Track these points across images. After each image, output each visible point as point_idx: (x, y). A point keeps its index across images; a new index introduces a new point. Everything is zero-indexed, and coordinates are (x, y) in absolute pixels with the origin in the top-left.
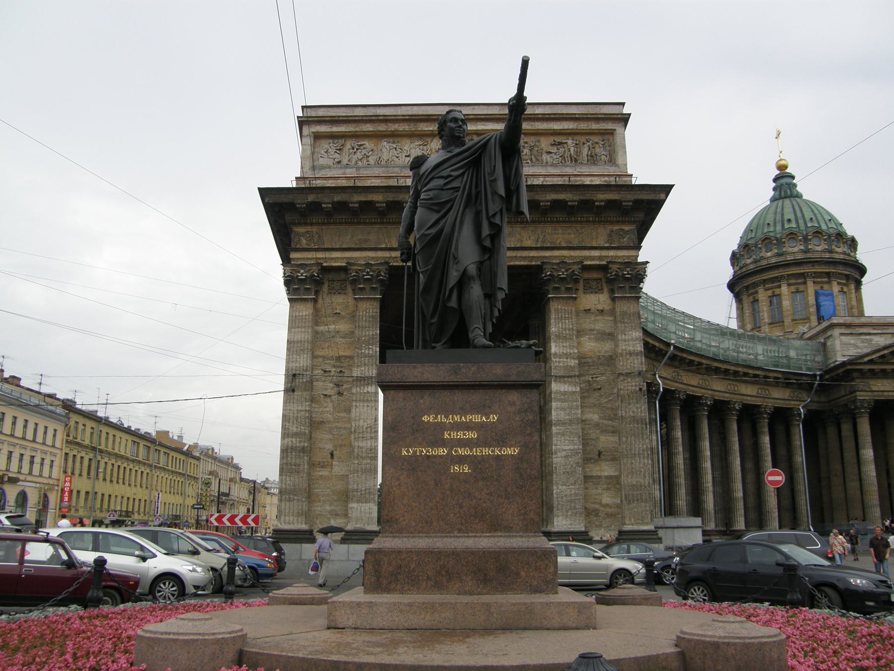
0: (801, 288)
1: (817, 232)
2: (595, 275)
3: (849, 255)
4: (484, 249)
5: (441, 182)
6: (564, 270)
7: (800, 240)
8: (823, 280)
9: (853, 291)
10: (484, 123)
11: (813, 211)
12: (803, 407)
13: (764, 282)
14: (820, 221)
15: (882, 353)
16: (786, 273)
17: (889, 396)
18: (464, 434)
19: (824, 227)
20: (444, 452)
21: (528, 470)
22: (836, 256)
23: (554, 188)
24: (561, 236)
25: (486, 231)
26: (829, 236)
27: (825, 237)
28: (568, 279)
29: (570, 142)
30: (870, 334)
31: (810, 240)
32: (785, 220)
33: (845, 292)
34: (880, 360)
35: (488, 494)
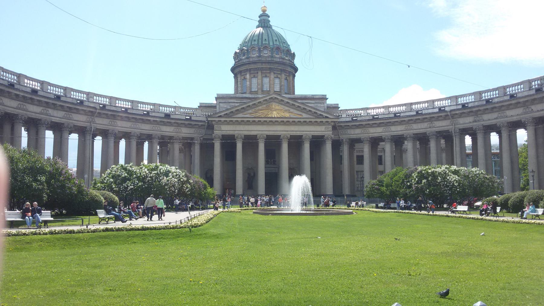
0: (256, 75)
1: (266, 47)
3: (284, 59)
7: (257, 51)
8: (267, 71)
11: (268, 35)
12: (200, 138)
13: (241, 72)
16: (249, 68)
17: (230, 133)
19: (271, 44)
22: (275, 60)
30: (234, 102)
31: (262, 51)
32: (253, 40)
33: (279, 78)
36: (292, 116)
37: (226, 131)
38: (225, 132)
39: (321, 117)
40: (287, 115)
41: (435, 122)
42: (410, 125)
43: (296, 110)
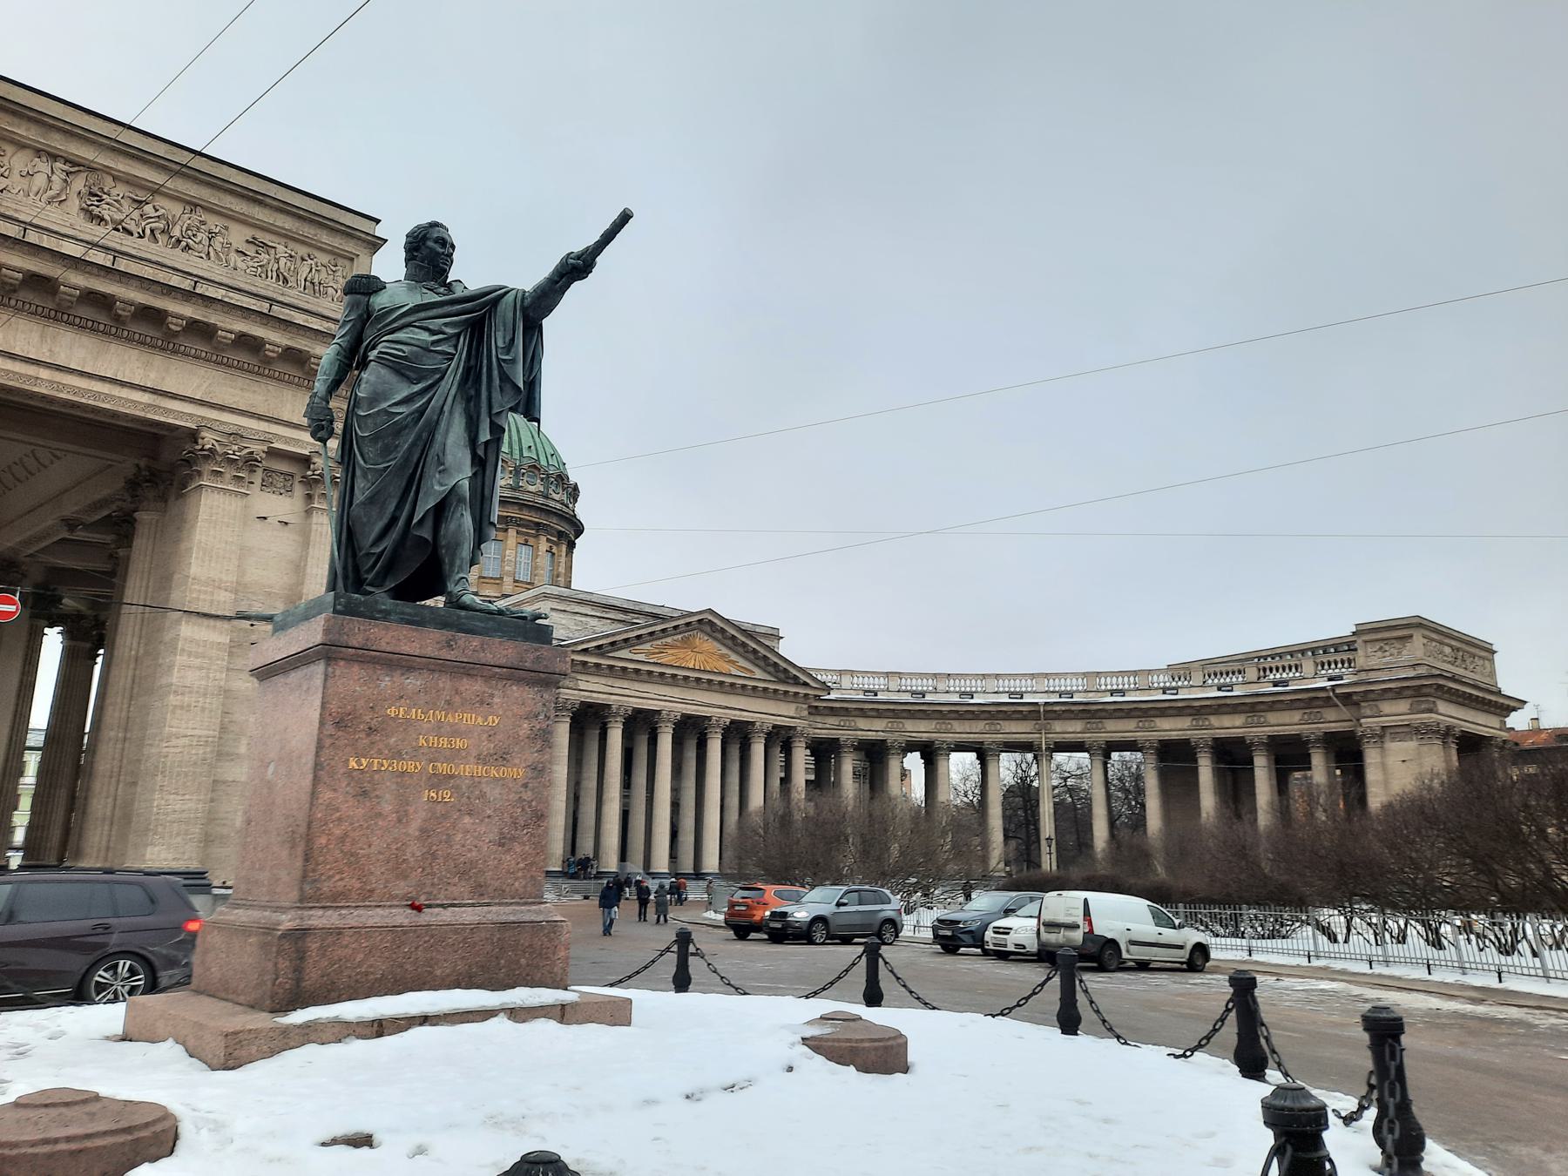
1: (535, 467)
2: (284, 467)
3: (568, 507)
4: (474, 455)
5: (425, 336)
6: (236, 448)
7: (511, 472)
9: (564, 554)
10: (130, 162)
14: (540, 453)
15: (600, 642)
17: (598, 698)
18: (450, 742)
19: (544, 462)
20: (416, 767)
21: (534, 803)
22: (552, 504)
23: (246, 312)
24: (240, 392)
25: (485, 436)
26: (548, 476)
27: (542, 476)
28: (240, 464)
29: (281, 248)
30: (587, 615)
33: (553, 554)
34: (597, 651)
35: (476, 838)
36: (734, 672)
37: (591, 691)
38: (586, 693)
39: (790, 681)
40: (726, 667)
41: (1000, 722)
42: (947, 721)
43: (743, 657)
